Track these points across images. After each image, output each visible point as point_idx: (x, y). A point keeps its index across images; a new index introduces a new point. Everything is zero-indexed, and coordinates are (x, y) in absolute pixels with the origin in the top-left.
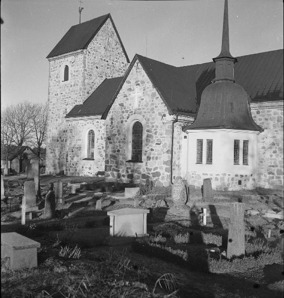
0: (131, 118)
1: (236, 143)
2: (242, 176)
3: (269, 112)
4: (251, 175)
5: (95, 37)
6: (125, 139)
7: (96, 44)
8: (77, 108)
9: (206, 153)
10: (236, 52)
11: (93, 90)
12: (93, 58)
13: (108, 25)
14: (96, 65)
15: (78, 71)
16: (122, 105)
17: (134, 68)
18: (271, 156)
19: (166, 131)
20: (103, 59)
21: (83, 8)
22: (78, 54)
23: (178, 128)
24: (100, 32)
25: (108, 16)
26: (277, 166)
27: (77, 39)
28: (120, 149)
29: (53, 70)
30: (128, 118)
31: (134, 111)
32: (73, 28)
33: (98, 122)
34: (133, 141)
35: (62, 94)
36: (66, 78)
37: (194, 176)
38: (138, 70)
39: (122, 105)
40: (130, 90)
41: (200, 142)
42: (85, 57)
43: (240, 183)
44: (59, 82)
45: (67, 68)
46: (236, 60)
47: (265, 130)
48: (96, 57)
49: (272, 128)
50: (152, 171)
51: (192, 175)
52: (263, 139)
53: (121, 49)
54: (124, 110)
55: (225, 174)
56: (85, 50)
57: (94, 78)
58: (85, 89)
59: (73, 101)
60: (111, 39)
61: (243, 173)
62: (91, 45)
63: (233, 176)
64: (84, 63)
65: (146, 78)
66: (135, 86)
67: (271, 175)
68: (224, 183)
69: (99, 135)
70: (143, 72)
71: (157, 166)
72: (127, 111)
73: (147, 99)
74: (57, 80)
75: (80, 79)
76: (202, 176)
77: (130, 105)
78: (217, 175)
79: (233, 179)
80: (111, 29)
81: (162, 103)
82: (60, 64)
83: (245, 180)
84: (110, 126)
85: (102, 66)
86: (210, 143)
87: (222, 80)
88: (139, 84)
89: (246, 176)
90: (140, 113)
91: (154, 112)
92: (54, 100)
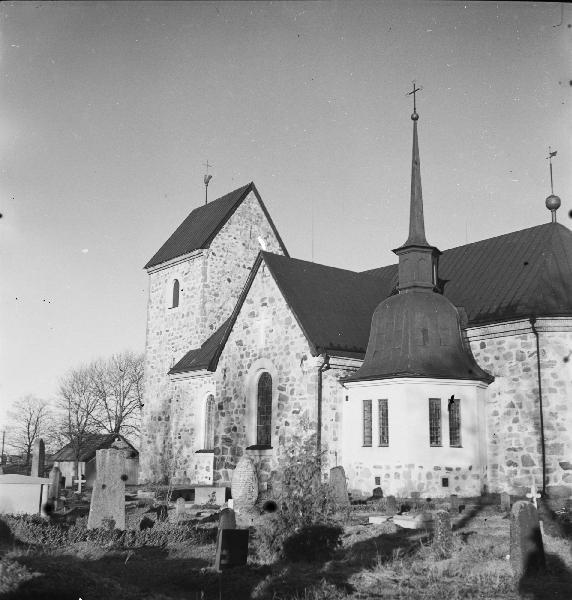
0: (256, 365)
1: (434, 406)
2: (449, 469)
3: (500, 343)
4: (470, 468)
5: (225, 226)
6: (244, 406)
7: (227, 237)
8: (191, 355)
9: (378, 427)
10: (444, 236)
11: (222, 322)
12: (221, 263)
13: (250, 203)
14: (228, 276)
15: (193, 288)
16: (239, 343)
17: (258, 276)
18: (510, 429)
19: (309, 386)
20: (242, 264)
21: (210, 177)
22: (192, 258)
23: (330, 381)
24: (235, 217)
25: (251, 187)
26: (521, 449)
27: (198, 232)
32: (194, 211)
34: (259, 409)
36: (176, 303)
37: (359, 470)
38: (264, 279)
39: (239, 343)
40: (252, 315)
41: (368, 404)
42: (205, 263)
43: (445, 482)
44: (164, 310)
45: (177, 283)
46: (435, 252)
47: (497, 379)
48: (228, 262)
49: (508, 374)
51: (356, 470)
52: (494, 396)
53: (277, 244)
55: (411, 466)
56: (205, 251)
57: (223, 299)
58: (206, 320)
59: (185, 344)
60: (255, 228)
61: (453, 464)
62: (217, 242)
63: (429, 468)
64: (204, 273)
65: (277, 292)
67: (512, 468)
68: (410, 483)
70: (272, 282)
73: (279, 329)
74: (161, 307)
75: (197, 302)
76: (372, 470)
78: (399, 467)
79: (429, 476)
80: (255, 210)
81: (301, 336)
83: (457, 478)
84: (223, 383)
85: (239, 277)
86: (384, 404)
87: (409, 288)
88: (265, 304)
89: (458, 469)
90: (268, 357)
91: (288, 354)
92: (154, 344)
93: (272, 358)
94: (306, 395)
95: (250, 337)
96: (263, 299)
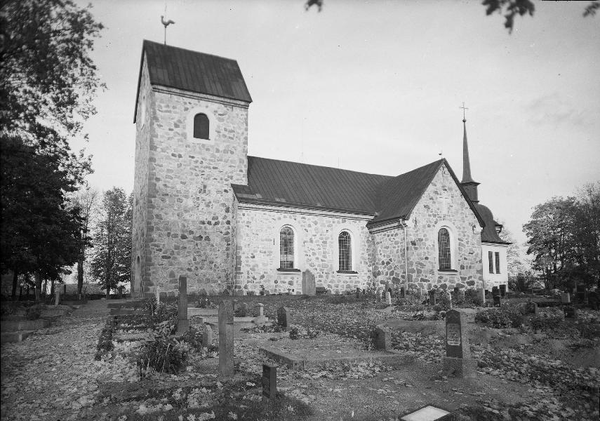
29: (164, 109)
30: (436, 223)
31: (442, 216)
33: (304, 218)
35: (193, 157)
41: (490, 253)
50: (467, 280)
66: (443, 191)
72: (435, 216)
82: (188, 106)
90: (450, 220)
91: (464, 222)
94: (476, 246)
95: (437, 205)
96: (443, 187)
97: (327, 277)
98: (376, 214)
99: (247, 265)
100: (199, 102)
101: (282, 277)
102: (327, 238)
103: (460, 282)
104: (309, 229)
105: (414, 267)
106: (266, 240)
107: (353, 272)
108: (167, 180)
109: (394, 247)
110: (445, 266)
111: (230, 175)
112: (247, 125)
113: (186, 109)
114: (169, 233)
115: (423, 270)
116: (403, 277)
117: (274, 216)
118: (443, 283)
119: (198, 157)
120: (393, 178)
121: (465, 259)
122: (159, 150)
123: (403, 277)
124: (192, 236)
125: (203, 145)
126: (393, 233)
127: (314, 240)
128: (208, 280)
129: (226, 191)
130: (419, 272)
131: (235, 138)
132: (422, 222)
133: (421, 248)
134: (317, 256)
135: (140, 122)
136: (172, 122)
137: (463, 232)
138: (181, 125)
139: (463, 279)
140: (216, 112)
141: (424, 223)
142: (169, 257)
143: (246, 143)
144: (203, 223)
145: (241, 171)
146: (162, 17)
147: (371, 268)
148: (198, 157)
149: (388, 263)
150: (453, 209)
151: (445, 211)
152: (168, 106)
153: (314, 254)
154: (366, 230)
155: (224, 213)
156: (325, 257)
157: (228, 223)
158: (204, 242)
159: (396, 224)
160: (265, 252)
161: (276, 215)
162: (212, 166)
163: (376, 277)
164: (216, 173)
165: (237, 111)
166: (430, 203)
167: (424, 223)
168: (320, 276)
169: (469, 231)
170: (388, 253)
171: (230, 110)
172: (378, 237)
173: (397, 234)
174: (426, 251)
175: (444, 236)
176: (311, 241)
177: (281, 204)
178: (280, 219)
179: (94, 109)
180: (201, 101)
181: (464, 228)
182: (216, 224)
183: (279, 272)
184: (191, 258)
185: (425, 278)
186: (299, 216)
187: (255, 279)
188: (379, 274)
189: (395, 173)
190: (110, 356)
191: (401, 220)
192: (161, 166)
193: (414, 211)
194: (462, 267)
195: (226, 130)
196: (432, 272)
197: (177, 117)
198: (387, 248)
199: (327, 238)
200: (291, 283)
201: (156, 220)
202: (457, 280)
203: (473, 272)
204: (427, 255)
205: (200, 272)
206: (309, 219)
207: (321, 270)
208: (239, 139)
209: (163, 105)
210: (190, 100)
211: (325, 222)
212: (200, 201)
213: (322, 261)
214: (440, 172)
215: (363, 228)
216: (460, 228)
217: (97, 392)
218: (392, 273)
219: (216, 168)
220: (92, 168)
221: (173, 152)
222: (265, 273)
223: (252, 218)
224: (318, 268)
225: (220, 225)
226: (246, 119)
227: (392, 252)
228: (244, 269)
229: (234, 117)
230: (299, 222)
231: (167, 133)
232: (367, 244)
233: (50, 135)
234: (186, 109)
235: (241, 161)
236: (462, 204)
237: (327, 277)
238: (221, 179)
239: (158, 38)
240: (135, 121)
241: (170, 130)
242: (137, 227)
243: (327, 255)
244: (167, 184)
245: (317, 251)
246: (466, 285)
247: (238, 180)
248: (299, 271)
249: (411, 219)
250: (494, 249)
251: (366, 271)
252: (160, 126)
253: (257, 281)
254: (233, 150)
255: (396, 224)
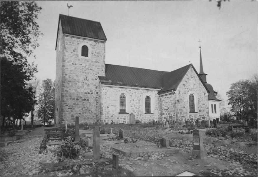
15: (98, 53)
19: (206, 99)
28: (185, 107)
29: (69, 44)
30: (188, 92)
31: (191, 89)
33: (130, 90)
35: (81, 65)
39: (184, 85)
41: (212, 105)
50: (202, 116)
54: (186, 88)
66: (191, 78)
69: (131, 98)
71: (203, 114)
72: (187, 89)
77: (189, 86)
82: (79, 42)
91: (200, 91)
93: (196, 91)
95: (188, 84)
96: (191, 76)
97: (140, 116)
98: (162, 88)
99: (105, 111)
100: (84, 40)
101: (121, 116)
102: (140, 99)
103: (199, 117)
104: (132, 95)
105: (179, 111)
106: (114, 100)
107: (152, 114)
108: (70, 74)
109: (170, 103)
110: (192, 110)
111: (97, 72)
112: (105, 50)
113: (78, 44)
114: (71, 98)
115: (182, 112)
116: (174, 115)
117: (117, 90)
118: (191, 118)
119: (84, 65)
120: (169, 72)
121: (201, 107)
122: (66, 62)
123: (174, 115)
124: (81, 99)
125: (86, 59)
126: (169, 96)
127: (135, 100)
128: (88, 118)
129: (96, 79)
130: (181, 113)
131: (99, 56)
132: (182, 91)
133: (182, 103)
134: (136, 107)
135: (58, 49)
136: (72, 49)
137: (200, 95)
138: (76, 51)
139: (200, 116)
140: (91, 45)
141: (183, 92)
142: (71, 108)
143: (104, 58)
144: (86, 93)
145: (103, 70)
146: (68, 4)
147: (160, 112)
148: (84, 65)
149: (167, 110)
150: (195, 86)
151: (192, 86)
152: (70, 43)
153: (135, 106)
154: (157, 95)
155: (95, 89)
156: (139, 107)
157: (97, 93)
158: (86, 102)
159: (171, 93)
160: (113, 106)
161: (118, 89)
162: (90, 69)
163: (162, 116)
164: (91, 71)
165: (100, 44)
166: (185, 83)
167: (183, 92)
168: (137, 116)
169: (203, 95)
170: (167, 105)
171: (98, 44)
172: (163, 98)
173: (171, 97)
174: (184, 104)
175: (192, 97)
176: (133, 100)
177: (120, 85)
178: (119, 91)
179: (38, 44)
180: (85, 40)
181: (200, 94)
182: (92, 93)
183: (119, 114)
184: (81, 108)
185: (183, 116)
186: (128, 90)
187: (109, 117)
188: (163, 114)
189: (170, 70)
190: (46, 152)
191: (173, 91)
192: (68, 69)
193: (179, 87)
194: (200, 111)
195: (95, 52)
196: (186, 113)
197: (74, 47)
198: (167, 103)
199: (140, 99)
200: (124, 119)
201: (65, 92)
202: (198, 116)
203: (204, 113)
204: (184, 106)
205: (85, 114)
206: (132, 91)
207: (137, 113)
208: (102, 57)
209: (68, 42)
210: (80, 40)
211: (139, 92)
212: (84, 84)
213: (138, 109)
214: (189, 70)
215: (156, 94)
216: (198, 94)
217: (40, 167)
218: (169, 114)
219: (91, 69)
220: (37, 70)
221: (72, 62)
222: (113, 114)
223: (107, 91)
224: (136, 112)
225: (93, 94)
226: (105, 48)
227: (169, 105)
228: (104, 113)
229: (99, 47)
230: (128, 92)
231: (70, 54)
232: (158, 102)
233: (19, 56)
234: (78, 44)
235: (102, 66)
236: (199, 83)
237: (140, 116)
238: (94, 74)
239: (66, 13)
240: (56, 50)
241: (71, 53)
242: (57, 96)
243: (140, 106)
244: (70, 76)
245: (136, 105)
246: (202, 118)
247: (101, 74)
248: (128, 113)
249: (177, 90)
250: (214, 103)
251: (157, 113)
252: (67, 51)
253: (110, 118)
254: (99, 61)
255: (171, 93)
